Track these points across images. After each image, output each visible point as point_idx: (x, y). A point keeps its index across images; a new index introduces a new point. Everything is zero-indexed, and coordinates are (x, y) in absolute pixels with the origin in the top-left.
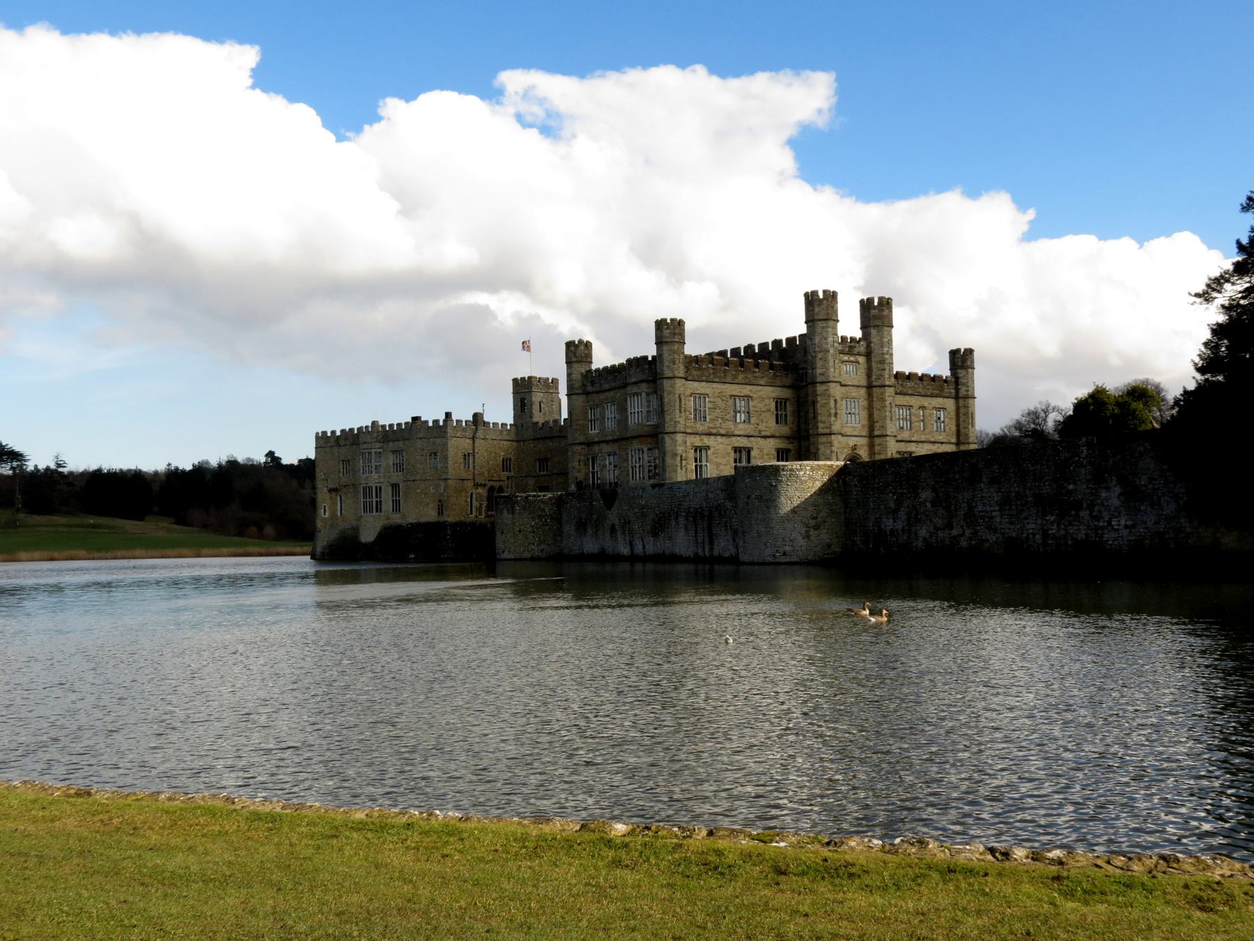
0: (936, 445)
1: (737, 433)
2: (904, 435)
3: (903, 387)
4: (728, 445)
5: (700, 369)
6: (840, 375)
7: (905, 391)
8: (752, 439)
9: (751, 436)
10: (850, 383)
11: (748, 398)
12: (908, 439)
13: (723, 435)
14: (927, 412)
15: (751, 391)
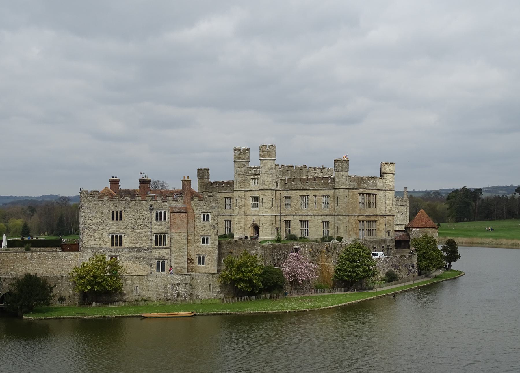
0: (323, 216)
1: (226, 214)
2: (304, 211)
3: (304, 185)
4: (223, 219)
5: (213, 187)
6: (249, 185)
7: (305, 187)
8: (232, 216)
9: (232, 215)
10: (254, 190)
11: (231, 198)
12: (306, 214)
13: (220, 215)
14: (317, 198)
15: (232, 194)
